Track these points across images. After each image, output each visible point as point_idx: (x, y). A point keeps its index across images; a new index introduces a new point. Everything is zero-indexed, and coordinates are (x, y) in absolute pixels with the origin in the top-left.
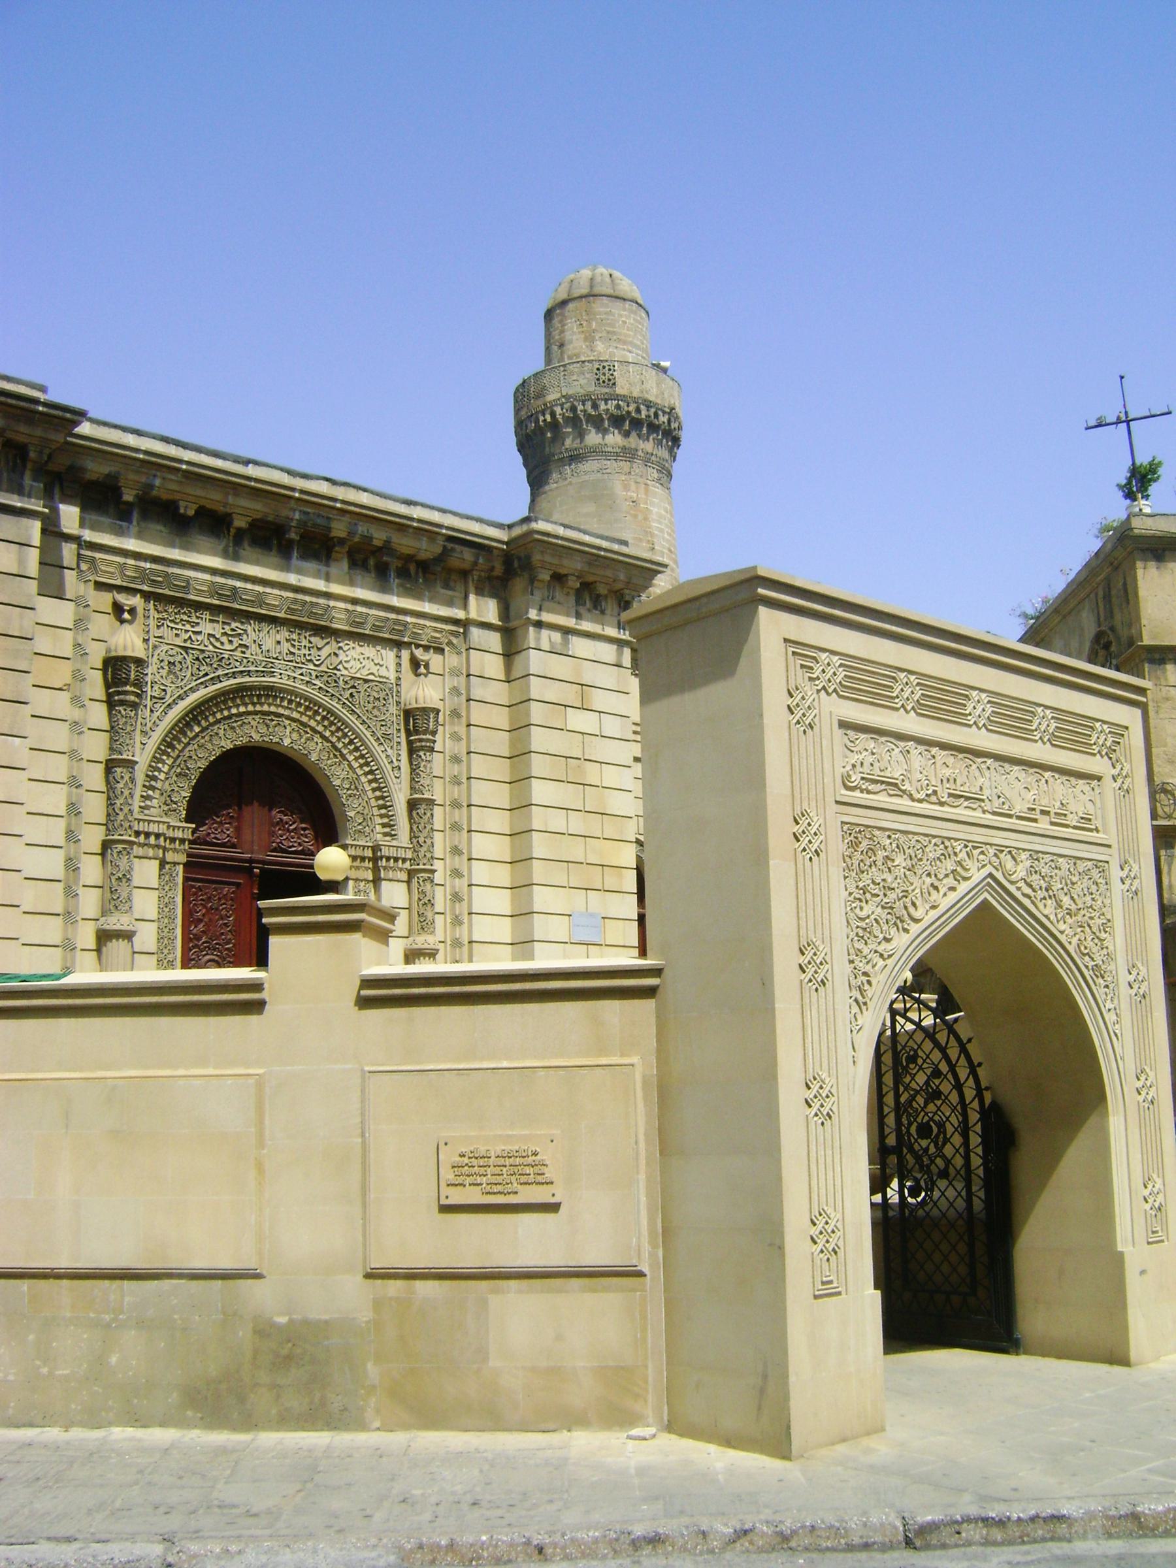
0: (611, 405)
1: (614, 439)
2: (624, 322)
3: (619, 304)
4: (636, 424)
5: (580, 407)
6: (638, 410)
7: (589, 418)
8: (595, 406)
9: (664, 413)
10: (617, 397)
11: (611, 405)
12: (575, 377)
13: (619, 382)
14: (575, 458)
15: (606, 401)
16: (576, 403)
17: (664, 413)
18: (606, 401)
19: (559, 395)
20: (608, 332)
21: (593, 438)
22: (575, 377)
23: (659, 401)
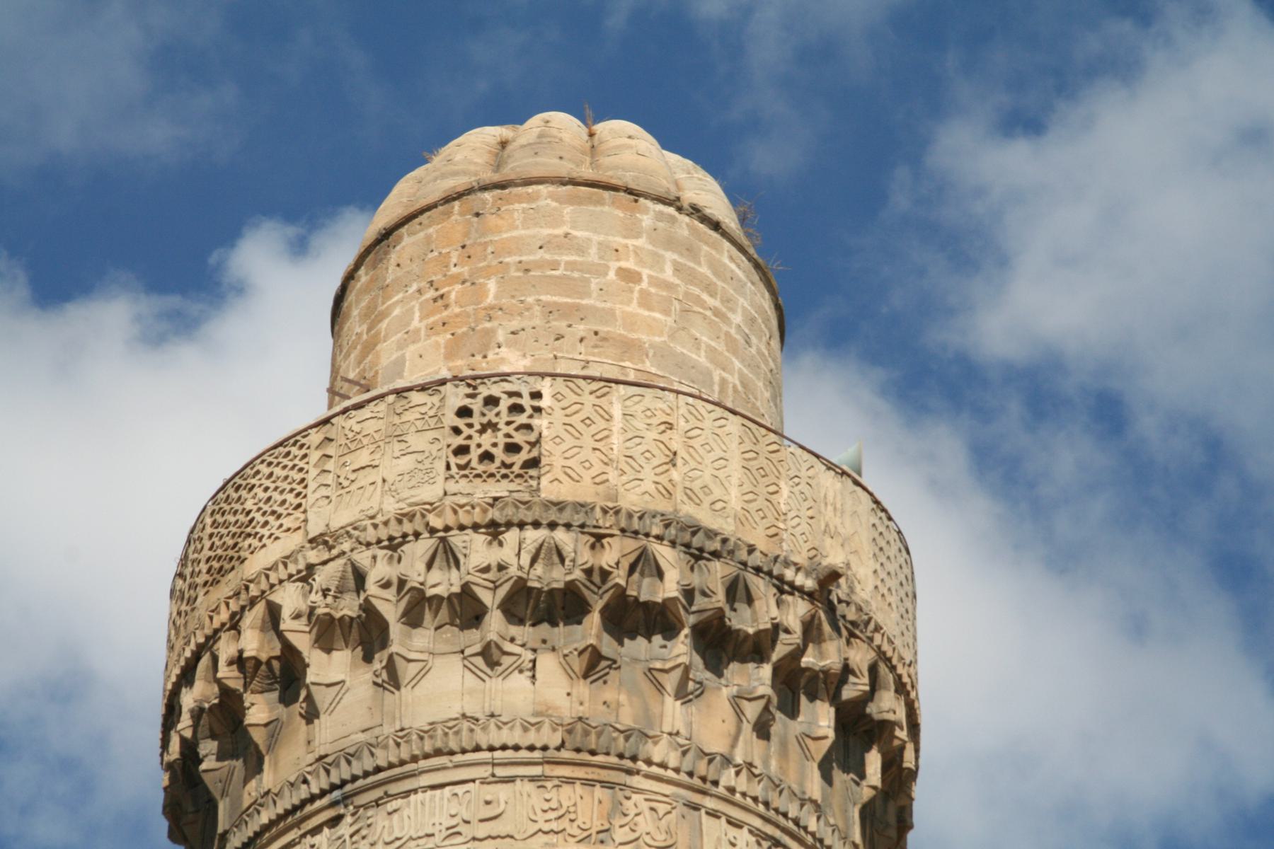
0: (514, 551)
1: (541, 686)
2: (629, 276)
3: (611, 209)
4: (634, 618)
5: (379, 569)
6: (644, 564)
7: (418, 606)
8: (447, 555)
9: (784, 588)
10: (556, 515)
11: (514, 551)
12: (363, 458)
13: (552, 453)
14: (352, 788)
15: (494, 530)
16: (362, 558)
17: (784, 588)
18: (494, 530)
19: (296, 540)
20: (550, 311)
21: (443, 684)
22: (363, 458)
23: (757, 537)
